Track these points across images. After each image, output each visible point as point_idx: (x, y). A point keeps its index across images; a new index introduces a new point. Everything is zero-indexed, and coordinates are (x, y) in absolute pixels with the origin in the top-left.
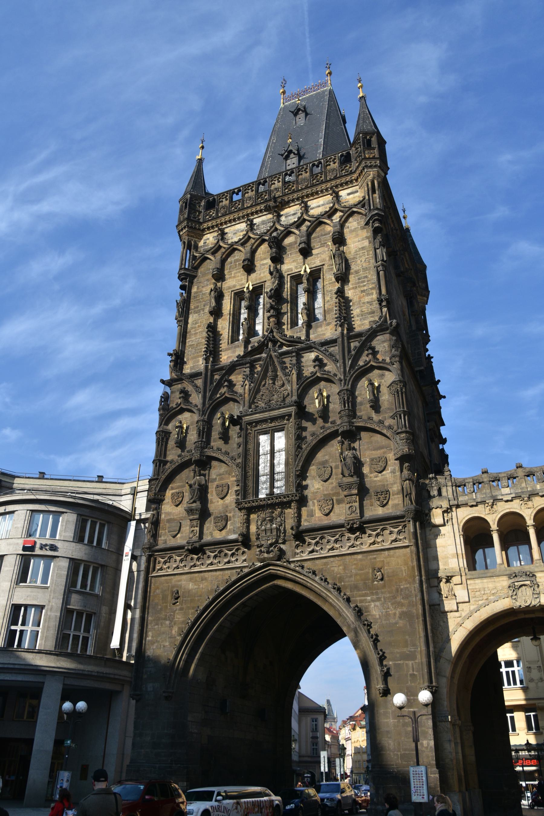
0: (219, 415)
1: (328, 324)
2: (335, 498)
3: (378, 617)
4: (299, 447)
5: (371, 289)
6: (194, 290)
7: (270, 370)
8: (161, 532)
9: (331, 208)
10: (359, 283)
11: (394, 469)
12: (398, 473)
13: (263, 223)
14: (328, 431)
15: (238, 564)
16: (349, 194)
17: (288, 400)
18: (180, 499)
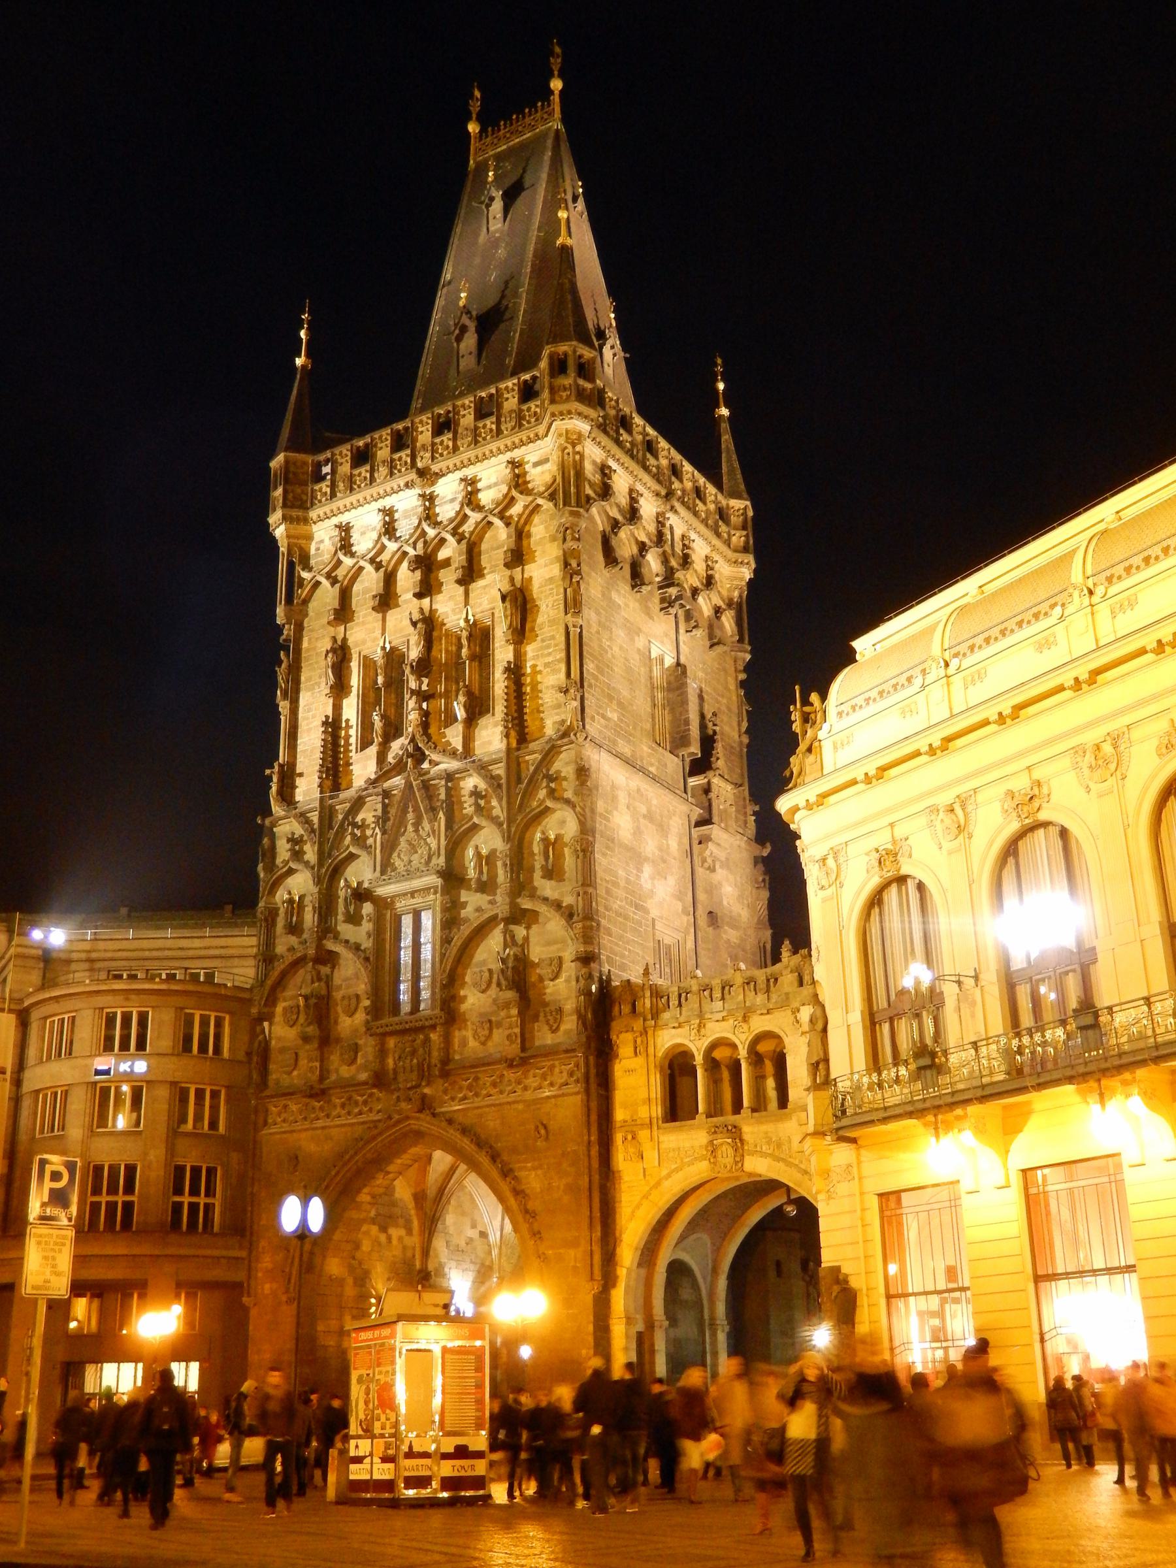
0: (342, 883)
1: (496, 725)
2: (493, 1019)
3: (538, 1190)
4: (446, 941)
5: (559, 661)
6: (305, 644)
7: (410, 810)
8: (272, 1067)
9: (505, 496)
10: (542, 648)
11: (570, 976)
12: (574, 983)
13: (407, 515)
14: (486, 916)
15: (373, 1117)
16: (536, 465)
17: (434, 861)
18: (294, 1017)
